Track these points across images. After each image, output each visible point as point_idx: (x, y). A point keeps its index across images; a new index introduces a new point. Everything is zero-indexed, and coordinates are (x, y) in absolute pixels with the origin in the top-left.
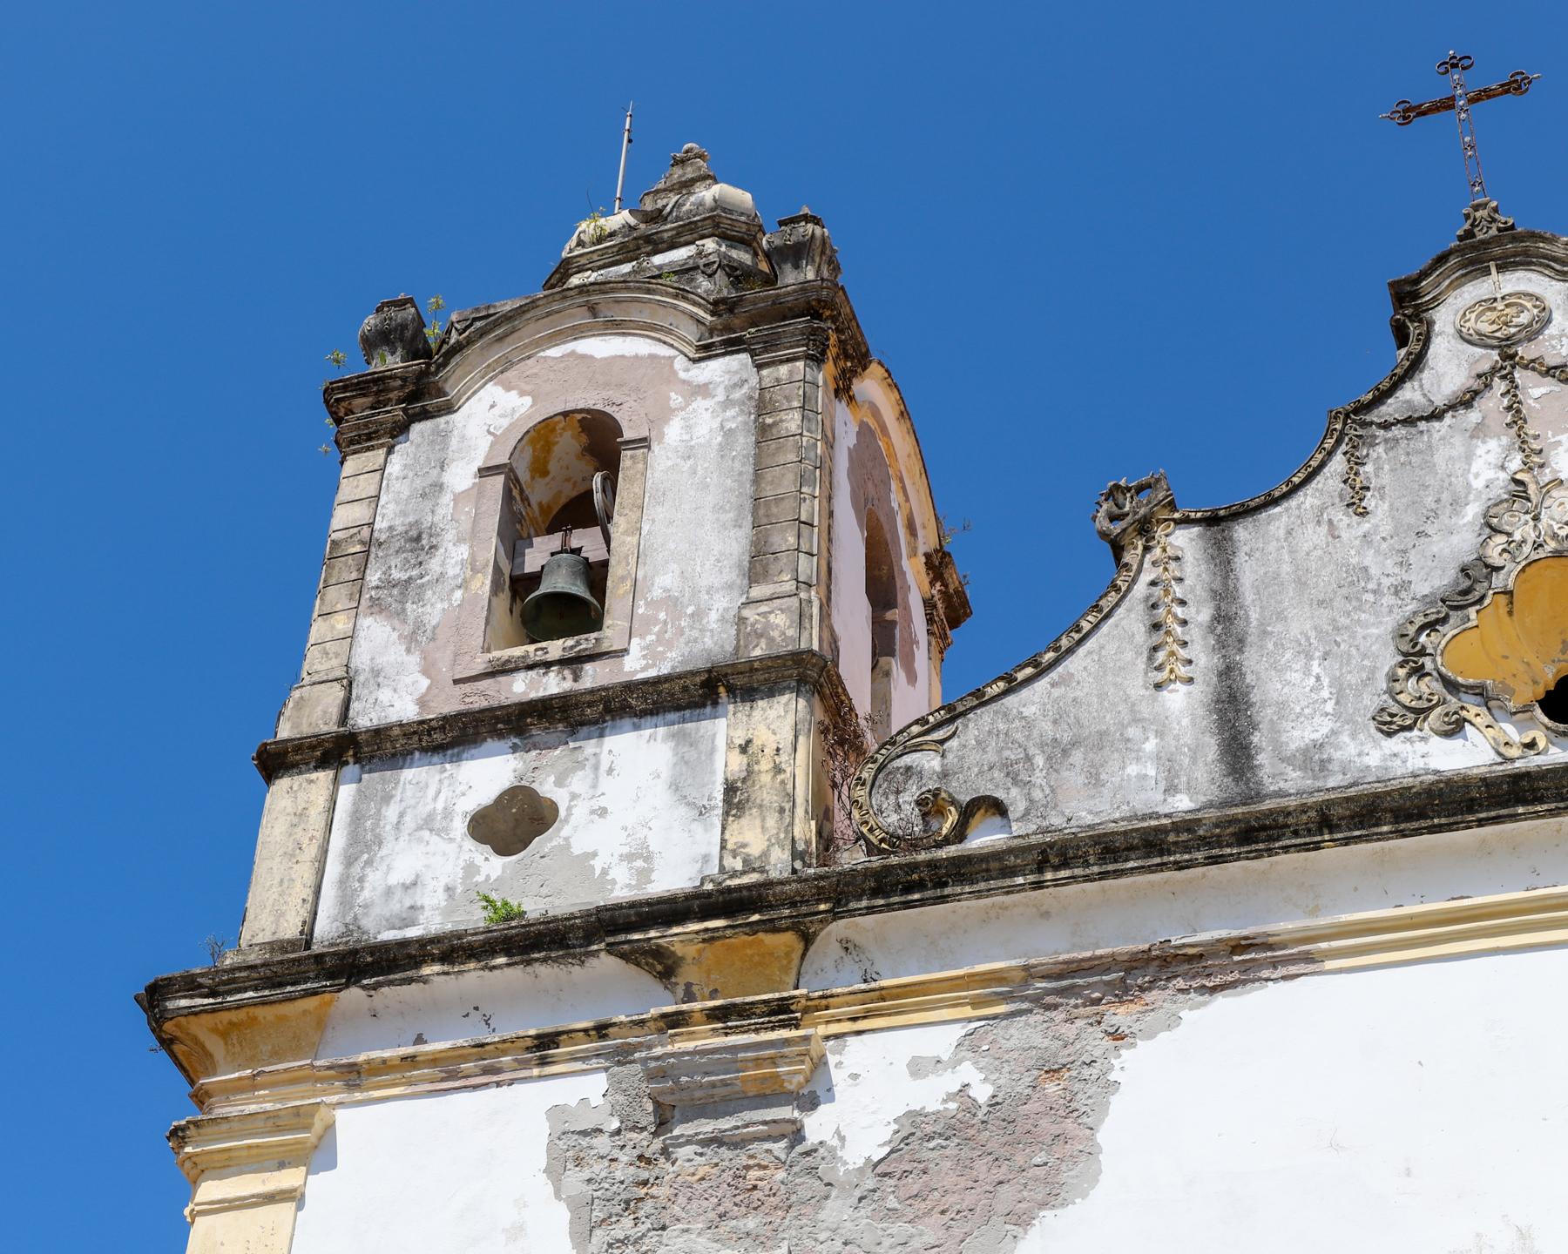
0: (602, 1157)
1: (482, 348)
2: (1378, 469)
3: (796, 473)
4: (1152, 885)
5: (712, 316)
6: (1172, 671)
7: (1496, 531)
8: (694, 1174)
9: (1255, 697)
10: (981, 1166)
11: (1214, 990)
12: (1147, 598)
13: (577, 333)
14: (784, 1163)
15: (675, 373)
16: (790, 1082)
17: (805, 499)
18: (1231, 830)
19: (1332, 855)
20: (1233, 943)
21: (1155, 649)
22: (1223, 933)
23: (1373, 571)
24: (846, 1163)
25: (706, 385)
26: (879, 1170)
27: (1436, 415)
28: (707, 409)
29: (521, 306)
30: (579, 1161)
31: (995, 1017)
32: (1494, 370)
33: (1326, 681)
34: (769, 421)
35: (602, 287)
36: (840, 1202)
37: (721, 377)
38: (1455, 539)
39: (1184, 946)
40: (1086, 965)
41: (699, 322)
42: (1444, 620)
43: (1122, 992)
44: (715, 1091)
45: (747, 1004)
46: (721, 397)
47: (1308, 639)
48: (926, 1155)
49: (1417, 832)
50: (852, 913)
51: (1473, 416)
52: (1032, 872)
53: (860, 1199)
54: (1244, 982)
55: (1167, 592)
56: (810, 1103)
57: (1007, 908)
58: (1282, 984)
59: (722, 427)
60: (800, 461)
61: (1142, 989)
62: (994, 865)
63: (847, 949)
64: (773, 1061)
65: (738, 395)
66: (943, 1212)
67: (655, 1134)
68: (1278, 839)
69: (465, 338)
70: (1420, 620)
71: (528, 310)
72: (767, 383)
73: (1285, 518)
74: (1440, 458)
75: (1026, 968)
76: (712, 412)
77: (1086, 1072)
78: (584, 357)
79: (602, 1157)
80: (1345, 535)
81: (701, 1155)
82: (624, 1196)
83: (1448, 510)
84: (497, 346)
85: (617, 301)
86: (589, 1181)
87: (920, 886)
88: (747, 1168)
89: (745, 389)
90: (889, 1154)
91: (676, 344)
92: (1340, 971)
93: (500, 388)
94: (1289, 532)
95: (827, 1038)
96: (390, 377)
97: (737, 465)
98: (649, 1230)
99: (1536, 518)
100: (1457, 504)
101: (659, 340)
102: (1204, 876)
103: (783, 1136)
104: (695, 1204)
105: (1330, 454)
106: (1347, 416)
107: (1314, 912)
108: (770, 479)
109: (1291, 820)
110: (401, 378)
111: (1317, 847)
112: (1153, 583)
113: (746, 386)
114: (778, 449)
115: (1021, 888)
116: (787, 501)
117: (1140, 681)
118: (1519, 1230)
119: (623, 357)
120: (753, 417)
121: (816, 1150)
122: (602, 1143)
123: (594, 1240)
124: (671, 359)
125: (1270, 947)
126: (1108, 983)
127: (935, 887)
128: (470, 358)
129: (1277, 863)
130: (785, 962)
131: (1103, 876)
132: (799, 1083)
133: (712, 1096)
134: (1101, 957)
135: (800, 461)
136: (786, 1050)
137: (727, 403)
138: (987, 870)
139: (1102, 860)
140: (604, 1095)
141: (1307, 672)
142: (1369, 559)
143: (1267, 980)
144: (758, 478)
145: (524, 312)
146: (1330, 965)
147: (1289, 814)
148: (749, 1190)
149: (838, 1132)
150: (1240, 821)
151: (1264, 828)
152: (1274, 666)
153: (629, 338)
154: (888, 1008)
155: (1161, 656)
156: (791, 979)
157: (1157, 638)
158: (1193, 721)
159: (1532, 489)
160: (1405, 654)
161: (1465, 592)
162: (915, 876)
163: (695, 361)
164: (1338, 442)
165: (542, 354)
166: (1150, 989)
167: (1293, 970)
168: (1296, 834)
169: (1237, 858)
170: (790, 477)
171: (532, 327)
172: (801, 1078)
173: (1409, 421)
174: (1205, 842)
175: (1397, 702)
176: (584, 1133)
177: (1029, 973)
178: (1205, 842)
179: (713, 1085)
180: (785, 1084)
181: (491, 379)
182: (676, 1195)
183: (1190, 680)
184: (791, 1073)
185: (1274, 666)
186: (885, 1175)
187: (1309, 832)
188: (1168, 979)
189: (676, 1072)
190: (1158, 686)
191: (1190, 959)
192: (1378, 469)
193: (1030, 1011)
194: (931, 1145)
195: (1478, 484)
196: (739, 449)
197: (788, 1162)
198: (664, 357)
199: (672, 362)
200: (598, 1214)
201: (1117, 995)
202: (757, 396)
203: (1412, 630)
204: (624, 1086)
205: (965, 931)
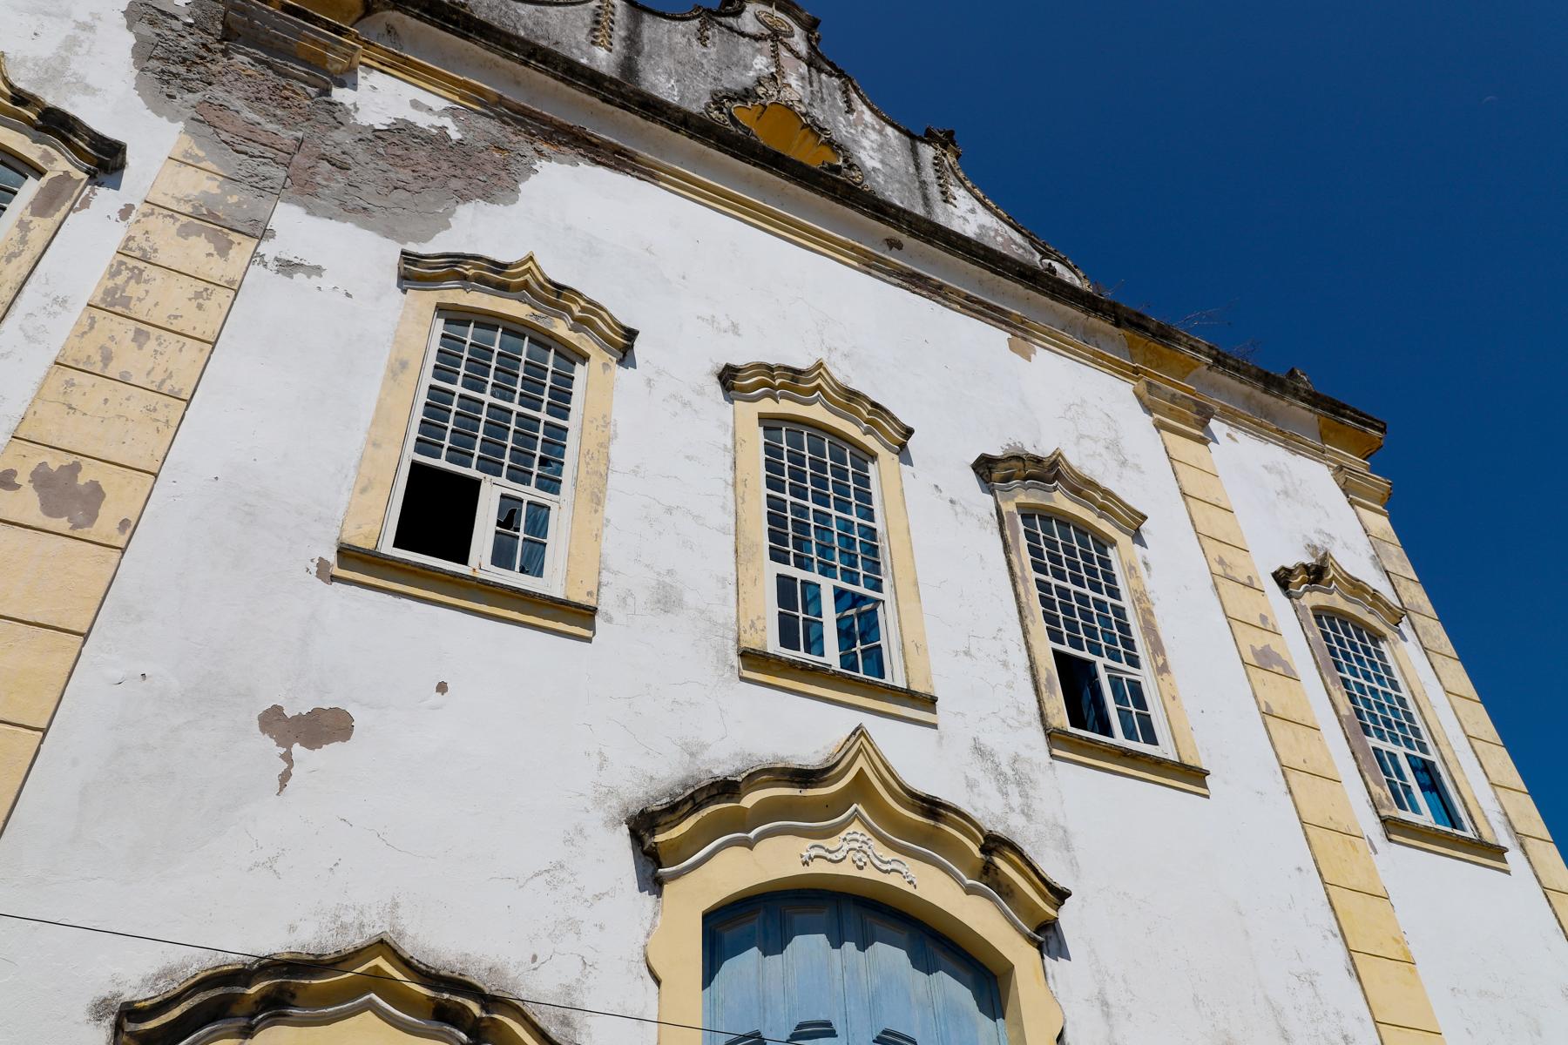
0: (173, 30)
2: (714, 35)
4: (583, 101)
6: (602, 41)
7: (761, 85)
8: (244, 71)
9: (641, 74)
10: (445, 165)
11: (599, 163)
12: (594, 11)
14: (312, 99)
16: (331, 66)
18: (637, 98)
19: (681, 139)
20: (616, 148)
21: (595, 30)
22: (615, 141)
23: (705, 66)
24: (356, 120)
26: (377, 133)
27: (743, 34)
30: (152, 23)
31: (472, 109)
32: (769, 35)
33: (676, 90)
36: (345, 134)
38: (743, 78)
39: (592, 135)
40: (533, 115)
42: (735, 100)
43: (548, 139)
44: (276, 42)
45: (316, 16)
47: (671, 70)
48: (408, 142)
49: (726, 152)
50: (406, 12)
51: (758, 45)
52: (523, 55)
53: (360, 140)
54: (616, 169)
55: (606, 13)
56: (342, 85)
57: (498, 66)
58: (635, 179)
61: (559, 142)
62: (504, 39)
63: (389, 32)
64: (326, 47)
66: (413, 171)
67: (219, 42)
68: (660, 116)
70: (724, 94)
73: (668, 25)
74: (742, 49)
75: (500, 97)
77: (519, 158)
79: (173, 30)
80: (695, 47)
81: (253, 65)
82: (184, 55)
83: (742, 67)
86: (158, 35)
87: (456, 23)
88: (285, 88)
90: (386, 130)
92: (666, 189)
94: (669, 31)
95: (361, 63)
98: (198, 79)
99: (779, 92)
100: (748, 67)
102: (613, 112)
103: (316, 87)
104: (239, 84)
105: (694, 18)
106: (704, 10)
107: (661, 157)
109: (669, 112)
111: (677, 131)
112: (599, 7)
115: (514, 59)
117: (584, 36)
118: (733, 323)
121: (336, 105)
122: (177, 25)
123: (151, 62)
125: (633, 160)
126: (542, 130)
127: (464, 29)
129: (651, 128)
130: (346, 15)
131: (563, 80)
132: (337, 70)
133: (272, 43)
134: (545, 116)
136: (338, 47)
138: (499, 39)
139: (565, 72)
140: (186, 4)
141: (669, 81)
142: (704, 61)
143: (628, 173)
146: (661, 183)
147: (670, 108)
148: (282, 97)
149: (355, 104)
150: (642, 96)
151: (655, 107)
152: (653, 70)
154: (408, 70)
155: (597, 34)
156: (349, 24)
157: (595, 26)
158: (608, 66)
159: (779, 82)
160: (713, 99)
161: (744, 96)
162: (455, 17)
164: (698, 16)
166: (564, 145)
167: (642, 176)
168: (669, 119)
169: (636, 113)
172: (340, 67)
173: (731, 29)
174: (622, 96)
175: (709, 115)
176: (163, 13)
177: (501, 101)
178: (622, 96)
179: (277, 37)
180: (328, 65)
182: (226, 73)
183: (610, 51)
184: (335, 61)
185: (653, 70)
186: (380, 138)
187: (675, 122)
188: (576, 147)
189: (254, 16)
190: (593, 43)
191: (591, 143)
192: (714, 35)
193: (494, 119)
194: (415, 140)
195: (757, 67)
197: (316, 99)
200: (158, 52)
201: (545, 138)
203: (720, 95)
204: (204, 8)
205: (467, 65)
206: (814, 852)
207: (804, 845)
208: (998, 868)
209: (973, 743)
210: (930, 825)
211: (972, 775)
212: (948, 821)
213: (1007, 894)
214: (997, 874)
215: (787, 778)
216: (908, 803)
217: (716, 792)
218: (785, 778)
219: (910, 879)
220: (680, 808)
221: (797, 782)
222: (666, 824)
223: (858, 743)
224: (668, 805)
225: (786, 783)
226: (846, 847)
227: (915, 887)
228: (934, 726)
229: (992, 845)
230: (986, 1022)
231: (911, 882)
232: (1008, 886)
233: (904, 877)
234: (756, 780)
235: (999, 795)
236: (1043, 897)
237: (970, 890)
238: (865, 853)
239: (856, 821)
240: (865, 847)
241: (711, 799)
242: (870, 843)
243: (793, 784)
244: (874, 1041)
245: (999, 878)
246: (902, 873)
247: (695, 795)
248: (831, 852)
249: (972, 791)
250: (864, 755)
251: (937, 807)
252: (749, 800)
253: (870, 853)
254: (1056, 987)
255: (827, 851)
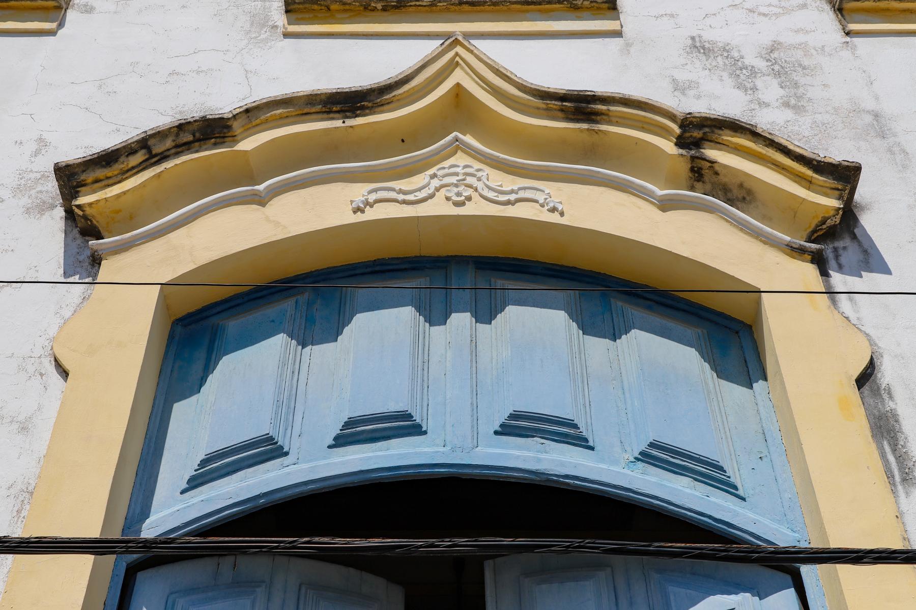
206: (372, 198)
207: (359, 191)
208: (712, 162)
209: (690, 42)
210: (581, 130)
211: (682, 76)
212: (614, 119)
213: (744, 198)
214: (717, 173)
215: (318, 108)
216: (538, 108)
217: (190, 138)
218: (313, 110)
219: (551, 205)
220: (121, 160)
221: (338, 112)
222: (97, 181)
223: (451, 54)
224: (96, 156)
225: (320, 116)
226: (435, 183)
227: (562, 214)
228: (618, 34)
229: (697, 134)
230: (733, 391)
231: (553, 210)
232: (741, 186)
233: (542, 206)
234: (263, 117)
235: (739, 94)
236: (808, 184)
237: (666, 205)
238: (470, 186)
239: (459, 153)
240: (470, 180)
241: (182, 148)
242: (479, 174)
243: (332, 115)
244: (496, 433)
245: (723, 179)
246: (536, 201)
247: (149, 143)
248: (405, 193)
249: (684, 94)
250: (462, 68)
251: (589, 102)
252: (248, 144)
253: (480, 185)
254: (856, 311)
255: (401, 192)
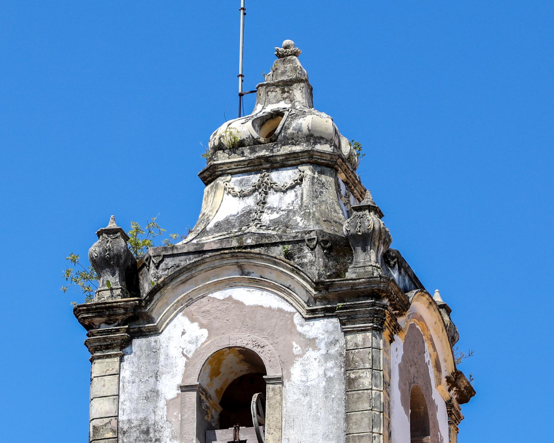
1: (173, 289)
3: (369, 419)
5: (315, 291)
13: (231, 284)
15: (294, 326)
17: (375, 437)
25: (314, 339)
28: (315, 359)
29: (195, 262)
34: (353, 376)
35: (246, 255)
37: (323, 334)
41: (307, 291)
46: (323, 351)
59: (325, 375)
60: (371, 410)
65: (334, 350)
69: (162, 282)
71: (200, 265)
72: (350, 346)
76: (319, 362)
78: (238, 303)
84: (182, 287)
85: (256, 265)
89: (337, 348)
91: (294, 304)
93: (187, 319)
96: (117, 307)
97: (335, 405)
101: (283, 298)
108: (355, 420)
110: (123, 308)
113: (338, 345)
114: (359, 398)
116: (365, 438)
119: (262, 307)
120: (343, 369)
124: (292, 314)
128: (166, 295)
135: (371, 410)
137: (327, 357)
144: (347, 419)
145: (197, 266)
153: (265, 293)
163: (307, 319)
165: (210, 295)
170: (366, 420)
171: (203, 275)
181: (180, 311)
196: (336, 393)
198: (287, 312)
199: (292, 317)
202: (345, 355)
